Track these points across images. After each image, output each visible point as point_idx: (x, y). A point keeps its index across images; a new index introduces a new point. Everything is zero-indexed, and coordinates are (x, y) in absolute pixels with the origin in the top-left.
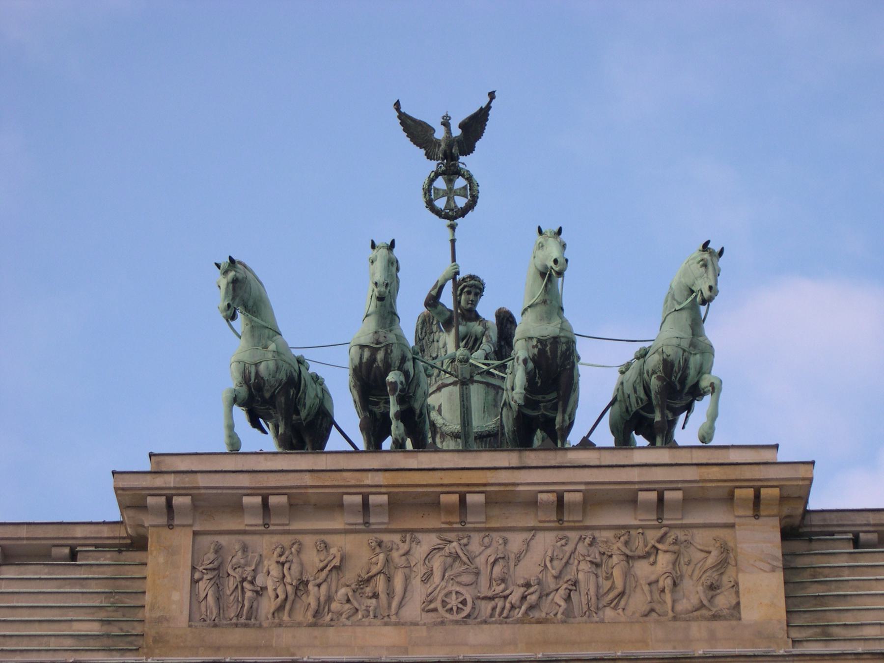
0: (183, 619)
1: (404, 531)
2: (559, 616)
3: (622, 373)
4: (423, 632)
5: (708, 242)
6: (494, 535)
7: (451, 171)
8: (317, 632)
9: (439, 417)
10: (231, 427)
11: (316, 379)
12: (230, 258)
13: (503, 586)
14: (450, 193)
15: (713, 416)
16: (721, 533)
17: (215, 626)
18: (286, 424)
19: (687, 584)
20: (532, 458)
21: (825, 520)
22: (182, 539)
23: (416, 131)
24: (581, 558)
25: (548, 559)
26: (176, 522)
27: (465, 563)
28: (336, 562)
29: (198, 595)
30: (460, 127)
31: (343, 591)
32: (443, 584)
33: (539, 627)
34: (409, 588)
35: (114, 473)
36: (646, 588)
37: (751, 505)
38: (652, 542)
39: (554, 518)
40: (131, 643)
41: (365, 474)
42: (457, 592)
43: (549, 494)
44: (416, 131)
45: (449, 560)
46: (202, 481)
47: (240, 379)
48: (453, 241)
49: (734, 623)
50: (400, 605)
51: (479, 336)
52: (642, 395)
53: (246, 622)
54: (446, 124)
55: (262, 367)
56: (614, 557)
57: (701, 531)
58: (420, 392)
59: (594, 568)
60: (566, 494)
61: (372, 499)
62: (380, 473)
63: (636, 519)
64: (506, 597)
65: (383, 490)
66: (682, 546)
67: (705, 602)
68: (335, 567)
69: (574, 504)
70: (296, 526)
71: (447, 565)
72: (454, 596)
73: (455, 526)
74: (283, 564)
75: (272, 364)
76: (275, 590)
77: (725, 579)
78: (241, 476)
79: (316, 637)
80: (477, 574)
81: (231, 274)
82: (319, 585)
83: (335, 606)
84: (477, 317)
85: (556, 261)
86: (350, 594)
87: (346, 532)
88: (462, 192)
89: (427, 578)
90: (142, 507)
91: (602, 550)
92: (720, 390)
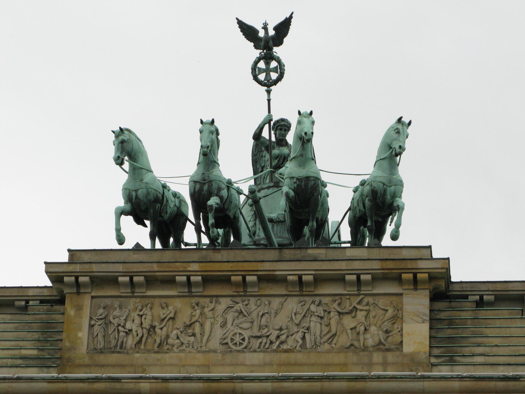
0: (83, 349)
2: (298, 348)
3: (354, 192)
5: (401, 118)
6: (263, 299)
7: (268, 57)
8: (159, 356)
10: (118, 230)
12: (120, 128)
13: (266, 330)
14: (268, 71)
16: (394, 298)
17: (102, 352)
21: (462, 288)
22: (87, 301)
23: (249, 32)
24: (313, 314)
26: (82, 291)
27: (245, 316)
28: (172, 315)
29: (93, 334)
30: (275, 29)
31: (175, 332)
33: (286, 355)
34: (213, 330)
35: (45, 263)
36: (349, 331)
37: (413, 283)
38: (354, 304)
40: (54, 363)
41: (188, 264)
42: (240, 334)
44: (249, 32)
46: (95, 268)
47: (127, 199)
48: (269, 101)
50: (208, 341)
51: (286, 156)
52: (362, 208)
53: (119, 350)
54: (265, 28)
55: (139, 192)
56: (331, 313)
58: (233, 205)
59: (319, 320)
61: (192, 278)
63: (345, 290)
64: (268, 336)
65: (199, 273)
66: (372, 307)
67: (383, 341)
68: (171, 318)
69: (308, 284)
70: (150, 293)
71: (235, 317)
72: (238, 335)
73: (241, 294)
74: (141, 316)
75: (144, 191)
76: (136, 331)
77: (396, 326)
78: (117, 265)
79: (158, 360)
81: (121, 138)
82: (161, 329)
83: (170, 341)
84: (286, 144)
85: (306, 133)
86: (179, 334)
88: (275, 70)
89: (224, 325)
91: (325, 309)
92: (403, 209)
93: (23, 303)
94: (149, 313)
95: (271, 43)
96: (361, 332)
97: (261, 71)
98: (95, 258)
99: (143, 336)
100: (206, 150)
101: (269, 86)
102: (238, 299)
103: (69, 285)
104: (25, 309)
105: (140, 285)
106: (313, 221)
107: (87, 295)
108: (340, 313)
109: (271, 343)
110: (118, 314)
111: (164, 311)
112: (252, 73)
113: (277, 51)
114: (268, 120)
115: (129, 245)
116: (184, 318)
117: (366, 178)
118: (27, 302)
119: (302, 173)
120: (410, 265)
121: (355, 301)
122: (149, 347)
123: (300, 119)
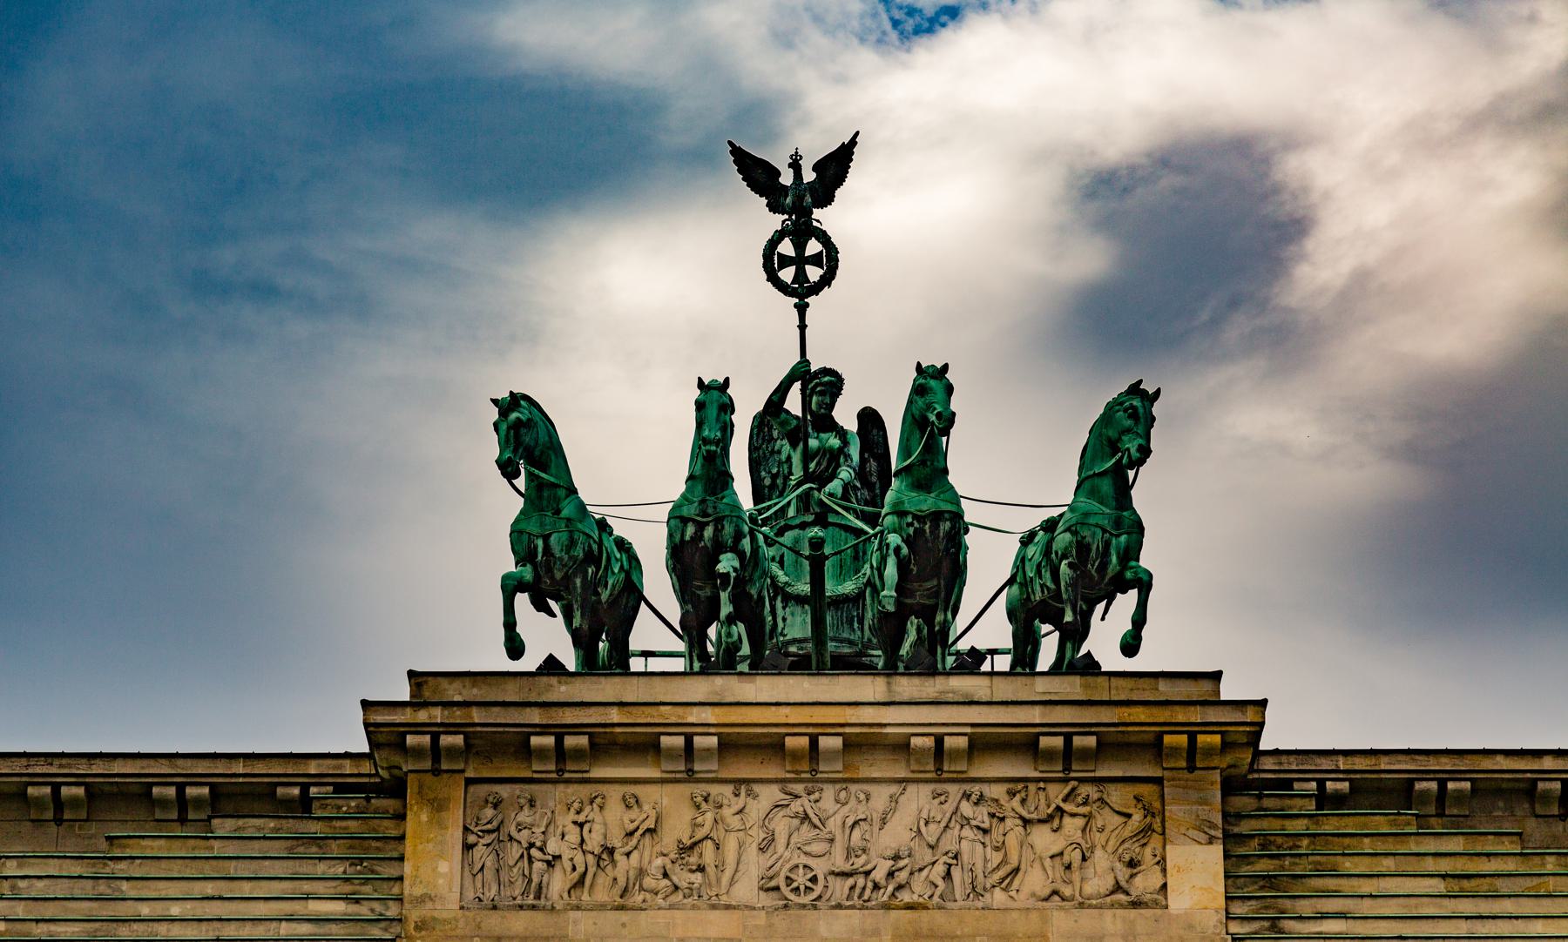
1: (738, 782)
2: (936, 899)
4: (761, 919)
6: (853, 788)
7: (802, 230)
8: (624, 916)
9: (780, 573)
10: (510, 625)
11: (622, 545)
13: (864, 857)
14: (800, 261)
15: (1139, 620)
16: (1146, 790)
17: (495, 908)
18: (582, 615)
19: (1101, 859)
20: (907, 687)
25: (922, 823)
27: (815, 827)
28: (650, 824)
30: (814, 169)
32: (787, 854)
35: (365, 704)
36: (1048, 862)
39: (931, 767)
40: (386, 930)
41: (689, 709)
42: (805, 866)
43: (925, 739)
45: (796, 822)
46: (477, 716)
48: (802, 327)
49: (1159, 912)
50: (732, 882)
54: (795, 165)
55: (553, 539)
57: (1120, 786)
59: (980, 836)
60: (946, 738)
62: (709, 709)
65: (712, 730)
67: (1123, 883)
68: (648, 830)
69: (956, 754)
70: (598, 772)
72: (801, 870)
74: (581, 825)
75: (565, 536)
77: (1148, 851)
79: (624, 925)
80: (832, 841)
82: (628, 854)
83: (648, 882)
87: (663, 781)
88: (816, 260)
90: (400, 746)
92: (1149, 586)
93: (296, 791)
94: (598, 819)
95: (808, 199)
96: (1075, 865)
97: (785, 261)
98: (474, 693)
99: (585, 873)
100: (713, 448)
101: (802, 297)
102: (799, 788)
103: (417, 752)
104: (304, 805)
105: (578, 754)
106: (945, 612)
107: (457, 776)
108: (1026, 822)
109: (876, 887)
110: (529, 820)
111: (634, 813)
112: (765, 266)
113: (823, 217)
114: (801, 373)
115: (530, 662)
116: (677, 828)
117: (1055, 512)
118: (305, 788)
119: (927, 503)
120: (1181, 716)
121: (1057, 792)
122: (601, 895)
123: (922, 381)
